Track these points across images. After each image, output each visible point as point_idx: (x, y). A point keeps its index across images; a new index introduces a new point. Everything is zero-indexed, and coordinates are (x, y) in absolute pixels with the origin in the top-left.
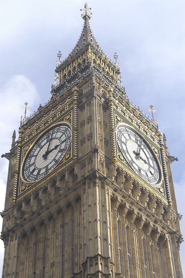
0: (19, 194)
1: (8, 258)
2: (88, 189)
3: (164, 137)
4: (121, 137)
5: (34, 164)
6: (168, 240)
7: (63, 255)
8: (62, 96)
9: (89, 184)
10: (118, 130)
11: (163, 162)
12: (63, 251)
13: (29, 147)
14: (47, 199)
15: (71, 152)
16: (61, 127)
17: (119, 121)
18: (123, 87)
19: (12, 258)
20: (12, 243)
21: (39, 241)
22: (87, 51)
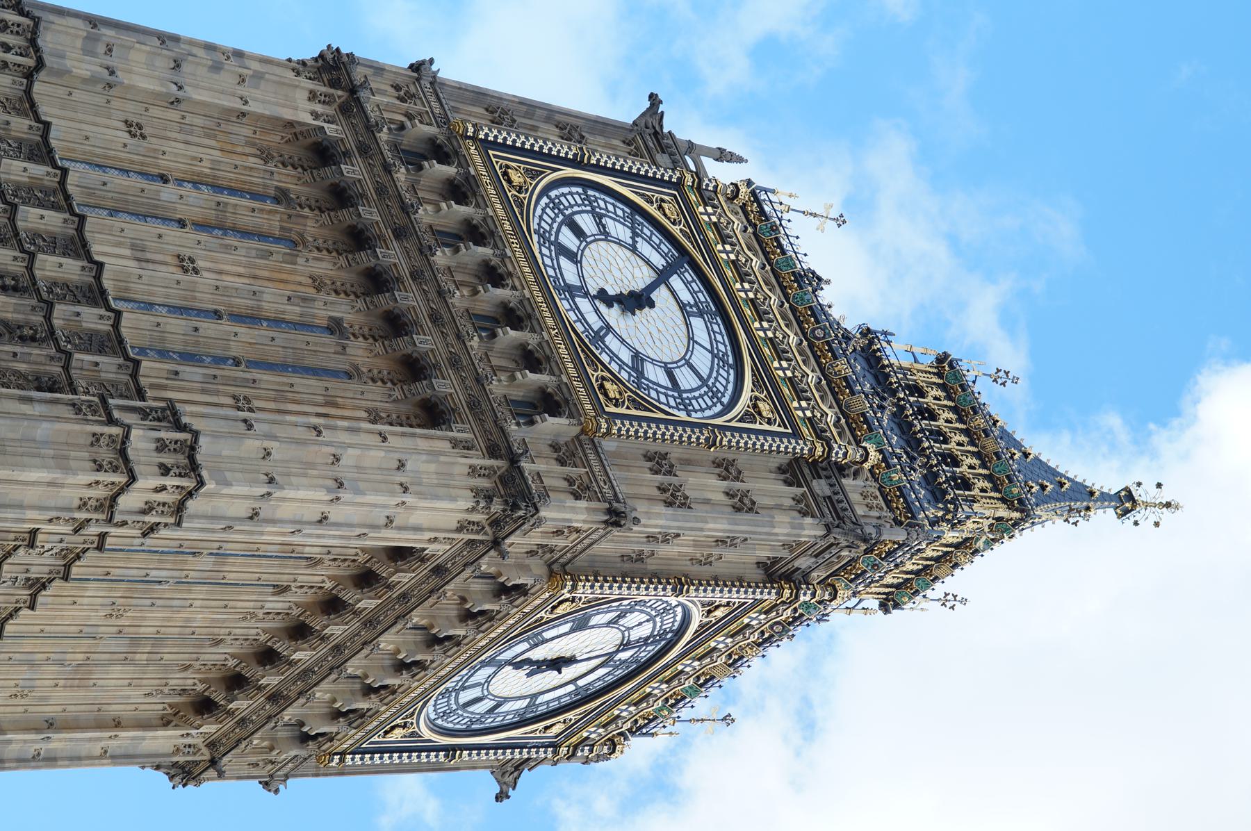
0: (495, 156)
1: (245, 71)
4: (642, 611)
5: (601, 234)
6: (193, 732)
7: (217, 315)
8: (849, 386)
10: (674, 603)
11: (505, 747)
12: (239, 318)
13: (674, 223)
14: (458, 277)
15: (628, 408)
16: (729, 374)
17: (709, 612)
19: (242, 91)
20: (301, 97)
21: (290, 217)
22: (1003, 500)
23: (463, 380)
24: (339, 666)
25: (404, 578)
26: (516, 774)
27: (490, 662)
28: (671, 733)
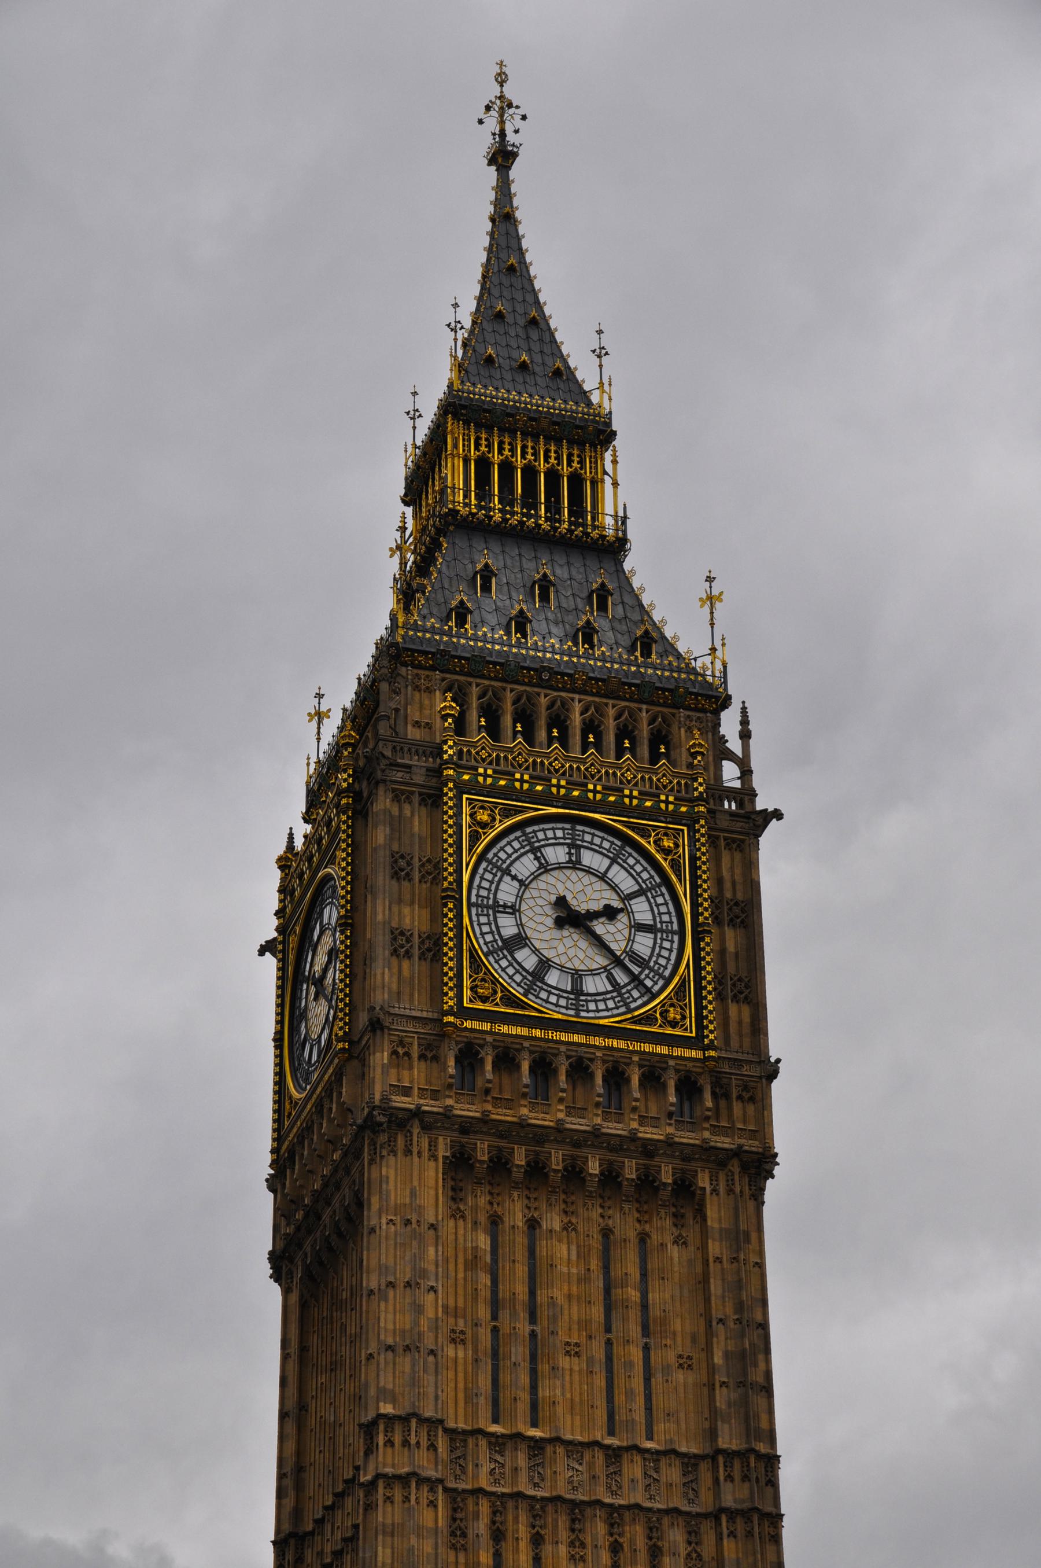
2: (370, 1164)
3: (745, 722)
4: (497, 889)
9: (372, 1147)
17: (484, 825)
18: (615, 516)
24: (595, 1132)
25: (482, 1150)
26: (753, 817)
27: (577, 991)
28: (723, 645)
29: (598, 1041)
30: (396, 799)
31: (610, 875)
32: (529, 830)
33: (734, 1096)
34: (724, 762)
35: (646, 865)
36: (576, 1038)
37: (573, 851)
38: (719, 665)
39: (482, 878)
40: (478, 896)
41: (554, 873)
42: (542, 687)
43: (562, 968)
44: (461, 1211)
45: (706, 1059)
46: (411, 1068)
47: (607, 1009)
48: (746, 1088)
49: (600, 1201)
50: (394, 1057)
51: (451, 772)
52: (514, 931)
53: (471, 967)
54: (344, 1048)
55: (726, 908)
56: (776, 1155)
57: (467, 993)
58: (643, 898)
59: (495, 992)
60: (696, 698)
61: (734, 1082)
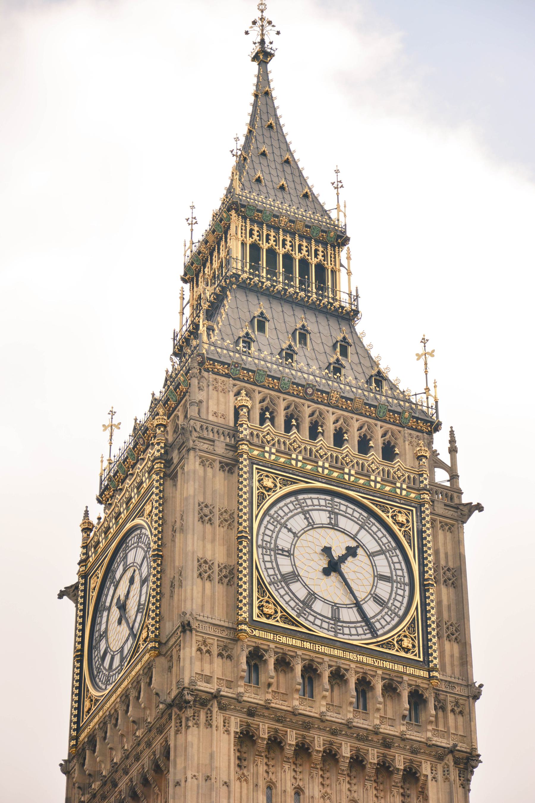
3: (452, 441)
4: (277, 537)
6: (430, 778)
9: (178, 721)
13: (98, 578)
17: (269, 489)
18: (350, 295)
23: (153, 739)
24: (349, 725)
25: (264, 729)
26: (461, 507)
27: (336, 619)
28: (435, 387)
29: (352, 656)
30: (202, 463)
31: (359, 536)
32: (300, 497)
33: (449, 708)
34: (436, 470)
35: (385, 533)
36: (336, 652)
37: (332, 516)
38: (432, 402)
39: (266, 528)
40: (263, 540)
41: (317, 530)
42: (307, 400)
43: (325, 601)
44: (245, 776)
45: (431, 678)
46: (211, 662)
47: (358, 635)
48: (457, 704)
49: (348, 779)
50: (199, 653)
51: (245, 447)
52: (290, 569)
53: (258, 592)
54: (155, 647)
55: (442, 572)
56: (479, 756)
57: (256, 611)
58: (383, 557)
59: (276, 612)
60: (417, 421)
61: (449, 699)
